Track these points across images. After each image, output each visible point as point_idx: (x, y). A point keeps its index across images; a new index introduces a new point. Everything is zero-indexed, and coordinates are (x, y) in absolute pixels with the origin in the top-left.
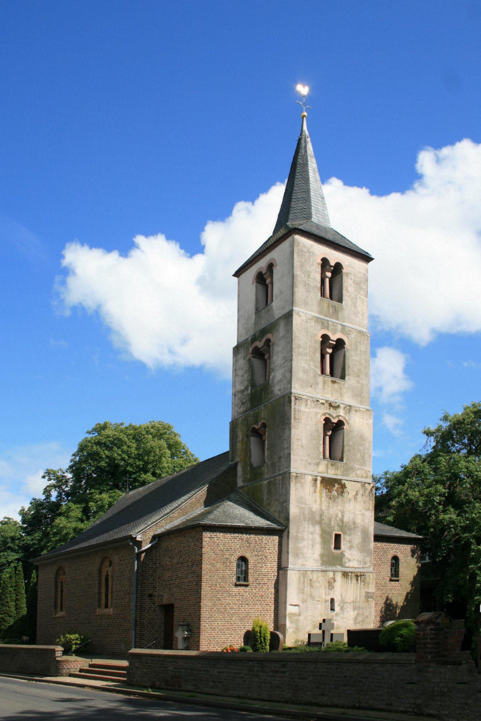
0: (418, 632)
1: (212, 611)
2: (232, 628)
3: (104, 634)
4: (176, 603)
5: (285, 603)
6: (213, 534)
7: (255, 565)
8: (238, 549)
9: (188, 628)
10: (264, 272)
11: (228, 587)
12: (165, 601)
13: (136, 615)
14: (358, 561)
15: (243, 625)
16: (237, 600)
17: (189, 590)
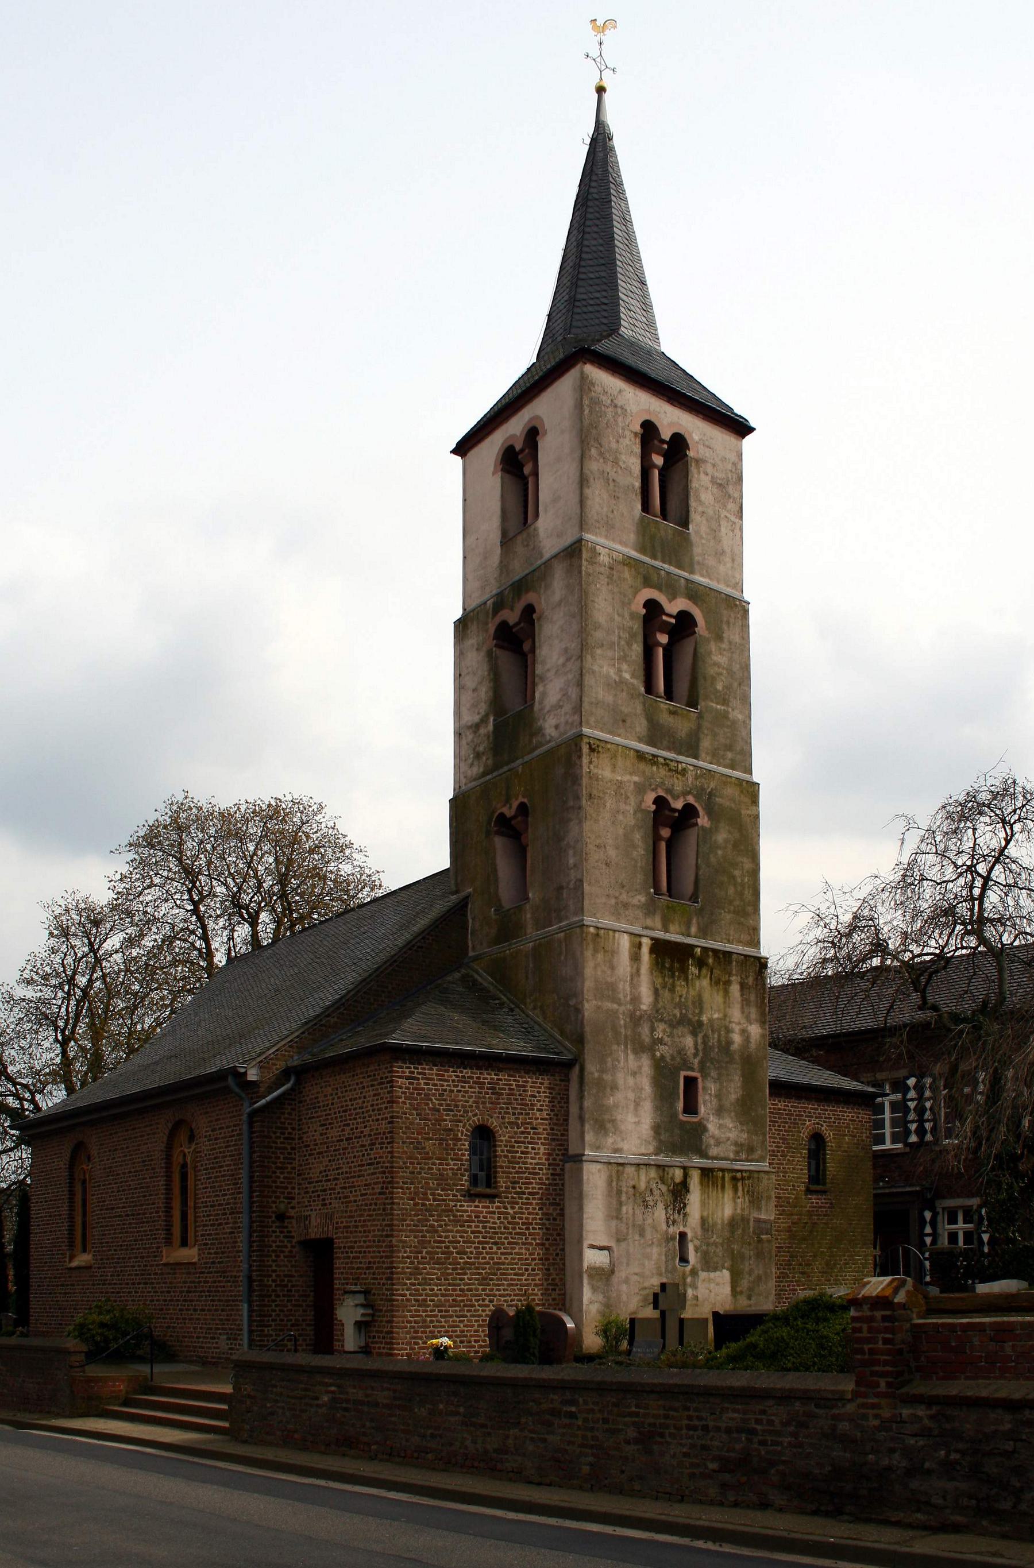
0: (857, 1325)
1: (417, 1258)
2: (463, 1301)
3: (181, 1310)
4: (339, 1238)
5: (580, 1241)
6: (416, 1070)
7: (510, 1147)
8: (471, 1106)
9: (365, 1299)
10: (518, 448)
11: (452, 1201)
12: (314, 1233)
13: (251, 1266)
14: (736, 1144)
15: (487, 1295)
16: (472, 1232)
17: (366, 1205)
